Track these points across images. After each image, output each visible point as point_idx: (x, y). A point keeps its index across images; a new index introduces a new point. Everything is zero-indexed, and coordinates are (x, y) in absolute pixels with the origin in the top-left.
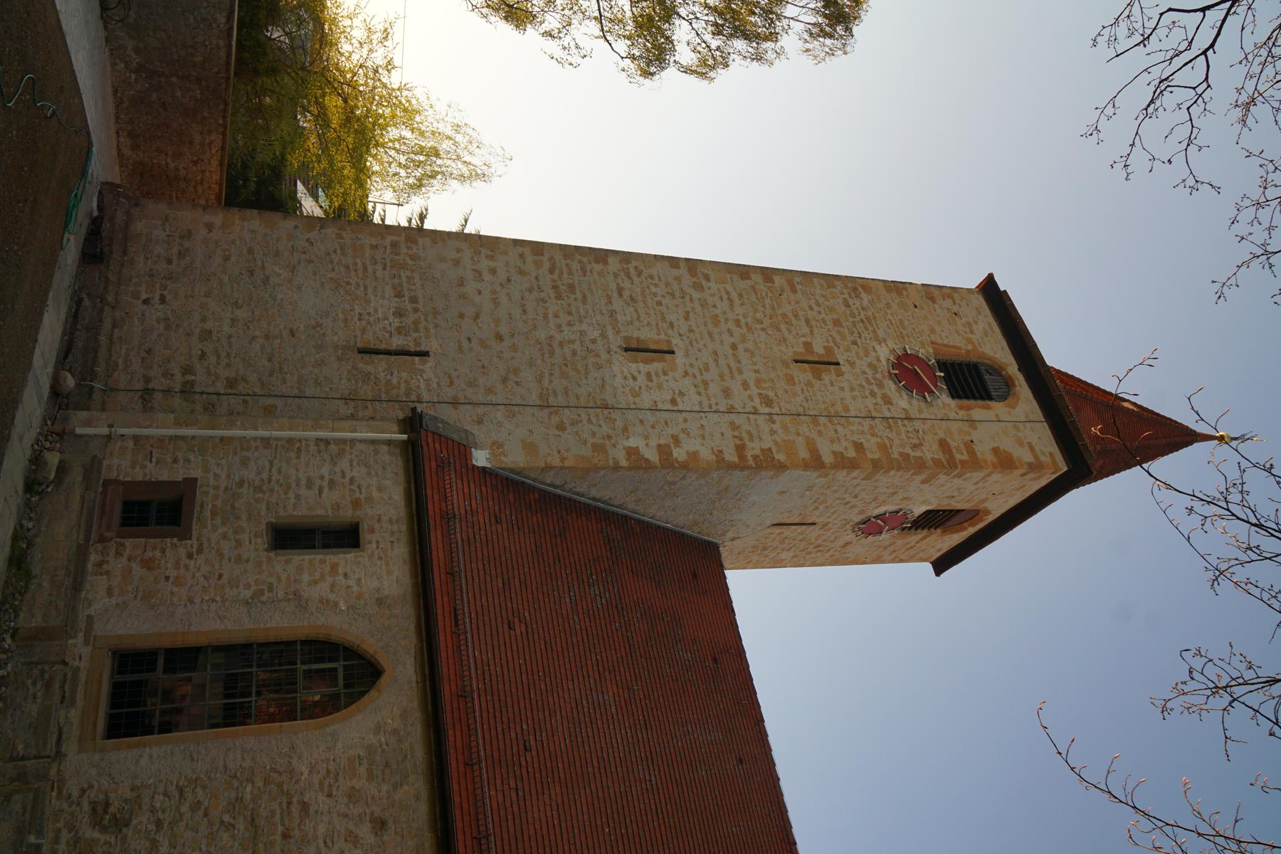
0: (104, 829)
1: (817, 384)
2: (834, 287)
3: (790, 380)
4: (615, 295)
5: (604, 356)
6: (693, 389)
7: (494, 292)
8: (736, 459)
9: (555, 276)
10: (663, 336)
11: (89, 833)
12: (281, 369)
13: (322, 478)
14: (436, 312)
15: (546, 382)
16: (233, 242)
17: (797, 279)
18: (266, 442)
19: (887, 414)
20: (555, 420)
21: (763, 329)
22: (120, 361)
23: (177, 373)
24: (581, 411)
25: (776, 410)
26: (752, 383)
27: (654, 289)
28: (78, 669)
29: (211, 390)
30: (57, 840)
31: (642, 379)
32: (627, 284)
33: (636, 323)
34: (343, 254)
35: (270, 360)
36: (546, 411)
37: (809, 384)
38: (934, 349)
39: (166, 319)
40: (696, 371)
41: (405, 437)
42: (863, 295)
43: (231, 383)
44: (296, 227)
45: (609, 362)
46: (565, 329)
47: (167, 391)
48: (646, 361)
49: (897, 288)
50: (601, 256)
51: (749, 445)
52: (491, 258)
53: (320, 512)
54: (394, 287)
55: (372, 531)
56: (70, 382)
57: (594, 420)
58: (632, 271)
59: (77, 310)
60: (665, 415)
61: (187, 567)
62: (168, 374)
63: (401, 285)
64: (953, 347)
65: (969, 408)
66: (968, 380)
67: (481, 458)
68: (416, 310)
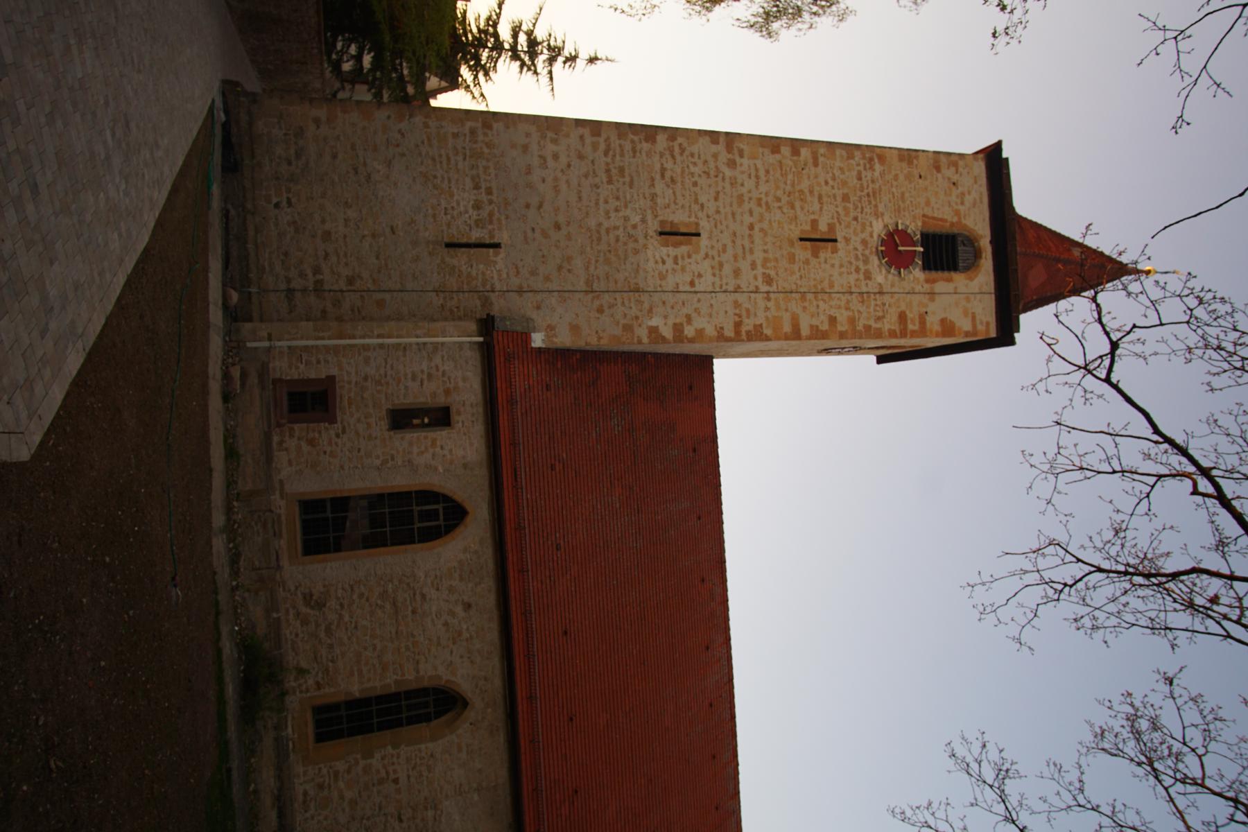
0: (312, 608)
1: (813, 261)
2: (853, 158)
3: (792, 258)
4: (658, 177)
5: (642, 241)
6: (710, 271)
7: (556, 179)
8: (732, 335)
9: (609, 160)
10: (693, 219)
11: (304, 610)
12: (386, 265)
13: (422, 371)
14: (507, 204)
15: (592, 269)
16: (338, 138)
17: (822, 151)
18: (381, 346)
19: (864, 289)
20: (597, 303)
21: (780, 208)
22: (266, 264)
23: (309, 272)
24: (618, 295)
25: (774, 288)
26: (759, 262)
27: (692, 169)
28: (279, 516)
29: (336, 287)
30: (287, 611)
31: (670, 262)
32: (669, 165)
33: (673, 206)
34: (430, 145)
35: (377, 258)
36: (590, 296)
37: (807, 262)
38: (924, 223)
39: (294, 222)
40: (715, 253)
41: (481, 339)
42: (877, 167)
43: (350, 281)
44: (389, 117)
45: (645, 246)
46: (613, 215)
47: (304, 290)
48: (676, 245)
49: (908, 156)
50: (649, 133)
51: (746, 321)
52: (555, 141)
53: (422, 400)
54: (473, 179)
55: (459, 413)
56: (235, 297)
57: (626, 302)
58: (677, 150)
59: (227, 224)
60: (683, 296)
61: (336, 444)
62: (302, 275)
63: (478, 176)
64: (941, 220)
65: (934, 281)
66: (941, 252)
67: (538, 340)
68: (491, 202)
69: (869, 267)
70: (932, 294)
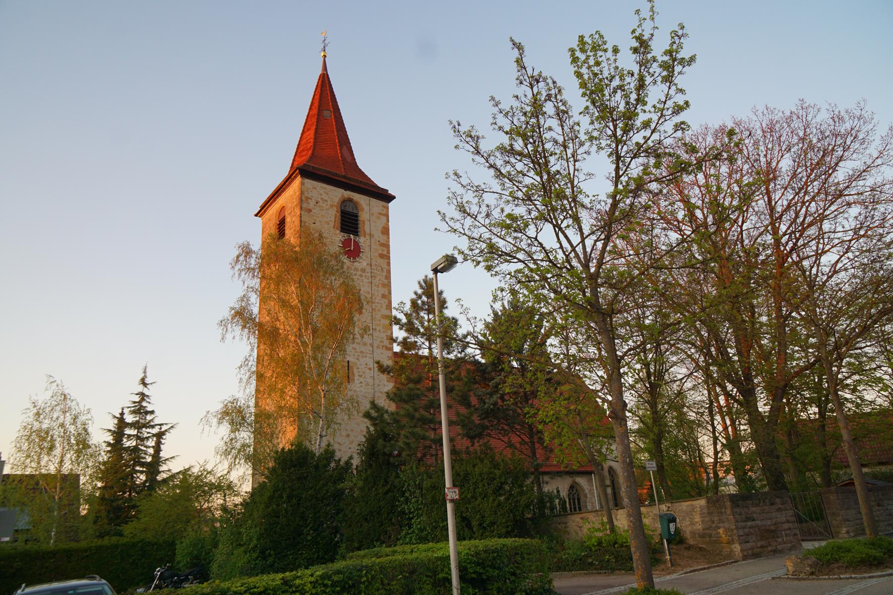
31: (362, 379)
40: (356, 354)
45: (355, 391)
69: (360, 268)
70: (371, 235)
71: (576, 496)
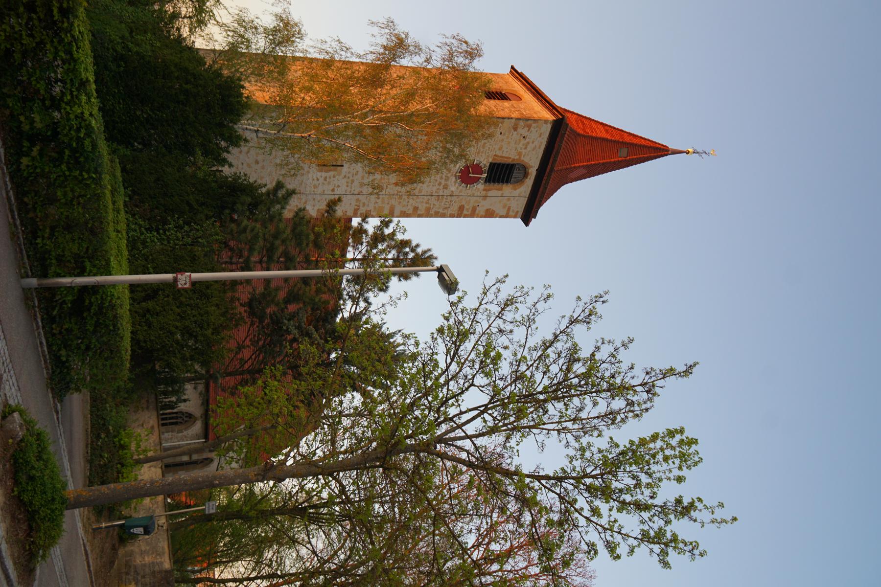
31: (321, 180)
40: (350, 175)
45: (308, 172)
48: (326, 172)
51: (361, 208)
65: (490, 190)
69: (448, 183)
70: (485, 197)
71: (179, 420)
